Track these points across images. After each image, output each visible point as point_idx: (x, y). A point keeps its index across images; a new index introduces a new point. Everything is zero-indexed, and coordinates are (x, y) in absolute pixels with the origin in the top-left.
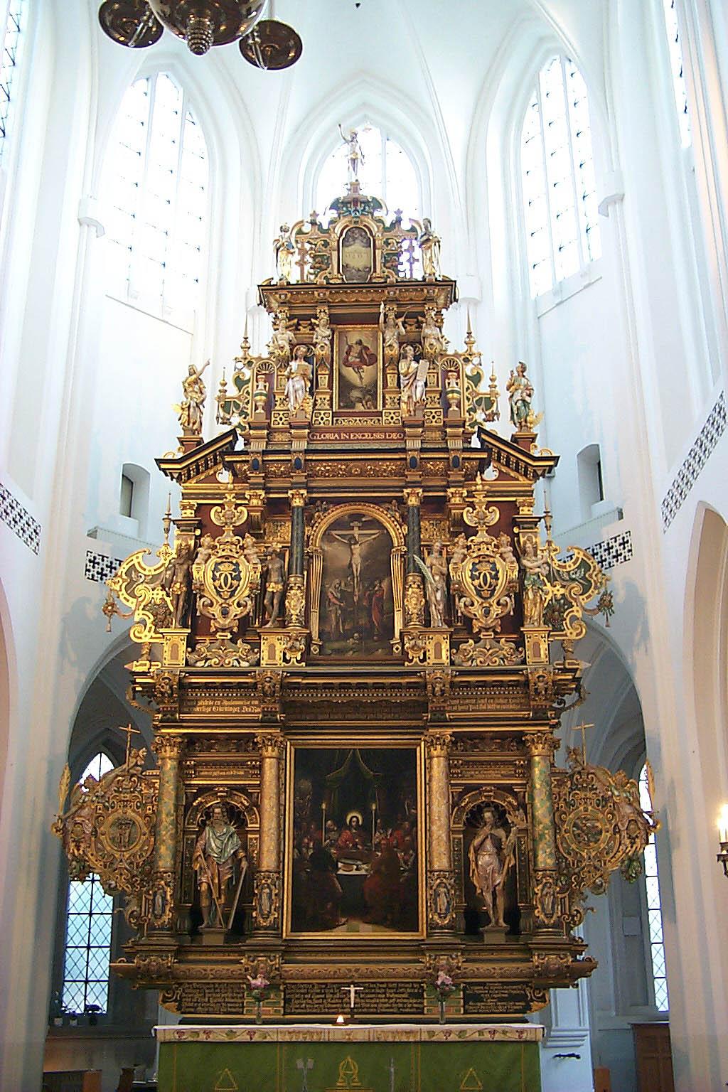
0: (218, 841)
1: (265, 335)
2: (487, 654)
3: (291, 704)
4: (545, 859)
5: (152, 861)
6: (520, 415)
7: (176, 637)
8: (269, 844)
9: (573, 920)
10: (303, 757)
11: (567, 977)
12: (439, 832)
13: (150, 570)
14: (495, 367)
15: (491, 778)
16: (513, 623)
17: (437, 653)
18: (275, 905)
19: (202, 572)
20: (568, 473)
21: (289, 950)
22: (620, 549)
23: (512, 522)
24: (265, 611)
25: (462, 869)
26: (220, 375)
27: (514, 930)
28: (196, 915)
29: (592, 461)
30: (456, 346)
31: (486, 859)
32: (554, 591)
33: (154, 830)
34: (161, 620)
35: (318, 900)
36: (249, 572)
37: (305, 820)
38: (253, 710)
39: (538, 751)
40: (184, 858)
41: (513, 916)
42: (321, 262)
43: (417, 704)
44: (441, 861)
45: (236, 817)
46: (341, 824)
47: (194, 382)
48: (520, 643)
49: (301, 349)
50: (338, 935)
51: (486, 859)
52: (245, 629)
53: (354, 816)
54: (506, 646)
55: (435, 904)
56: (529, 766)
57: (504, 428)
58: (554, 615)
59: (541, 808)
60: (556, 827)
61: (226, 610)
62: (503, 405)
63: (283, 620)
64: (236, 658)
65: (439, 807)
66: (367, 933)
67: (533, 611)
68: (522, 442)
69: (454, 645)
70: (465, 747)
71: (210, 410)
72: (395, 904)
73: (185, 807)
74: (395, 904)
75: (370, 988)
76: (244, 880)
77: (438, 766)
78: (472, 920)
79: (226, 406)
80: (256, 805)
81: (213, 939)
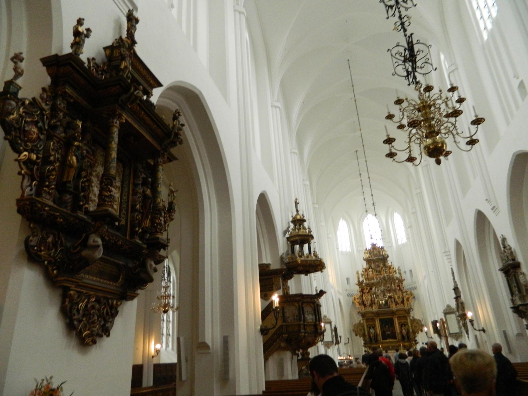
0: (372, 331)
1: (365, 265)
2: (400, 307)
3: (377, 314)
4: (411, 330)
5: (364, 333)
6: (400, 274)
7: (363, 307)
8: (378, 331)
9: (415, 337)
10: (380, 320)
13: (357, 297)
14: (396, 266)
16: (403, 302)
17: (394, 307)
18: (380, 338)
19: (364, 298)
21: (382, 343)
22: (415, 288)
24: (372, 303)
25: (401, 332)
26: (360, 272)
29: (411, 271)
30: (390, 264)
32: (407, 296)
33: (364, 329)
34: (360, 304)
35: (385, 337)
36: (369, 298)
37: (382, 327)
39: (408, 318)
42: (370, 254)
43: (393, 313)
44: (398, 331)
46: (385, 327)
47: (358, 273)
48: (404, 304)
49: (370, 267)
50: (388, 340)
51: (404, 331)
52: (371, 305)
53: (387, 326)
54: (402, 305)
56: (407, 319)
57: (398, 275)
58: (408, 299)
59: (410, 325)
60: (412, 326)
61: (368, 303)
62: (397, 271)
63: (375, 303)
64: (370, 309)
66: (391, 340)
67: (405, 300)
69: (396, 305)
70: (399, 318)
71: (360, 276)
72: (393, 336)
73: (367, 327)
74: (393, 336)
76: (376, 335)
77: (396, 320)
78: (403, 338)
79: (362, 275)
80: (375, 325)
81: (373, 342)
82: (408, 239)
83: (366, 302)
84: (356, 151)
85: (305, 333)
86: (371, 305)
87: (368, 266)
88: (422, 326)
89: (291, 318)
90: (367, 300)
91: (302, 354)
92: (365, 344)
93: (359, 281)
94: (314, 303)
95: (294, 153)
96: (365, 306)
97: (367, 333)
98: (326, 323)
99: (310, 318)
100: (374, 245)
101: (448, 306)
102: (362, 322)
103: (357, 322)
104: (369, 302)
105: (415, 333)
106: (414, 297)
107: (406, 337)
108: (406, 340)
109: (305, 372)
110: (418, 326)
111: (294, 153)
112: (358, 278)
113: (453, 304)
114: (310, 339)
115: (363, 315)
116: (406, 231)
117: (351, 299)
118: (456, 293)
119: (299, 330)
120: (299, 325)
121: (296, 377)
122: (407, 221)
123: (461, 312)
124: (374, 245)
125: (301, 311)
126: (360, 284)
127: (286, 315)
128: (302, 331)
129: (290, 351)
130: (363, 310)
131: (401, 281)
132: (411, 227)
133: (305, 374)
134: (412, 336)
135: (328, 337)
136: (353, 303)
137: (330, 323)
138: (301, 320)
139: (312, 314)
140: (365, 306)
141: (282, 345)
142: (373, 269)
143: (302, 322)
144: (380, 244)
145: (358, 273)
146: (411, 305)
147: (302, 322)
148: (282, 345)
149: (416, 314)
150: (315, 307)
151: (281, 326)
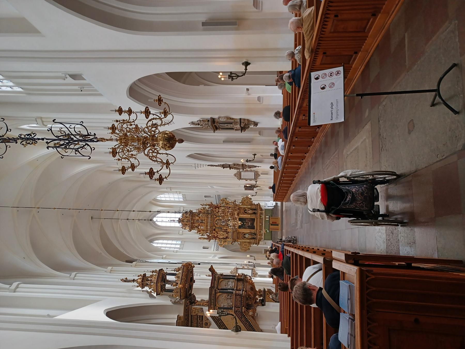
0: (247, 236)
4: (250, 207)
5: (248, 242)
6: (206, 205)
7: (228, 240)
11: (260, 206)
12: (247, 216)
14: (200, 207)
15: (242, 211)
19: (221, 237)
20: (206, 198)
21: (257, 230)
22: (219, 196)
23: (217, 207)
27: (255, 210)
28: (253, 238)
31: (249, 212)
34: (225, 242)
36: (222, 232)
38: (235, 232)
40: (248, 239)
41: (254, 210)
42: (186, 225)
44: (250, 216)
45: (244, 235)
47: (200, 238)
49: (197, 227)
51: (249, 212)
52: (228, 233)
55: (253, 216)
57: (207, 207)
59: (245, 206)
64: (230, 234)
65: (245, 216)
68: (209, 205)
71: (203, 237)
72: (253, 220)
74: (253, 220)
75: (260, 223)
77: (241, 215)
78: (254, 213)
79: (202, 235)
82: (180, 193)
83: (225, 237)
84: (92, 218)
85: (243, 290)
86: (228, 233)
87: (196, 229)
88: (247, 197)
89: (229, 301)
90: (223, 235)
91: (260, 296)
92: (256, 244)
93: (207, 239)
94: (219, 278)
95: (75, 276)
96: (227, 238)
97: (248, 241)
98: (237, 272)
99: (231, 284)
100: (180, 221)
101: (235, 175)
102: (239, 243)
103: (239, 247)
104: (225, 233)
105: (252, 204)
106: (226, 199)
107: (255, 211)
108: (256, 211)
109: (274, 296)
110: (247, 200)
111: (75, 276)
112: (205, 238)
113: (234, 171)
114: (249, 287)
115: (234, 241)
116: (173, 193)
117: (220, 248)
118: (227, 167)
119: (240, 295)
120: (236, 295)
121: (278, 304)
122: (166, 190)
123: (241, 167)
124: (180, 221)
125: (224, 291)
126: (209, 238)
127: (226, 306)
128: (241, 292)
129: (256, 307)
130: (230, 240)
131: (211, 205)
132: (171, 188)
133: (276, 296)
134: (254, 207)
135: (248, 273)
136: (223, 247)
137: (237, 269)
138: (232, 293)
139: (228, 282)
140: (227, 238)
141: (251, 313)
142: (199, 225)
143: (234, 292)
144: (179, 216)
145: (200, 238)
146: (231, 202)
147: (234, 292)
148: (251, 313)
149: (239, 201)
150: (222, 278)
151: (235, 312)
